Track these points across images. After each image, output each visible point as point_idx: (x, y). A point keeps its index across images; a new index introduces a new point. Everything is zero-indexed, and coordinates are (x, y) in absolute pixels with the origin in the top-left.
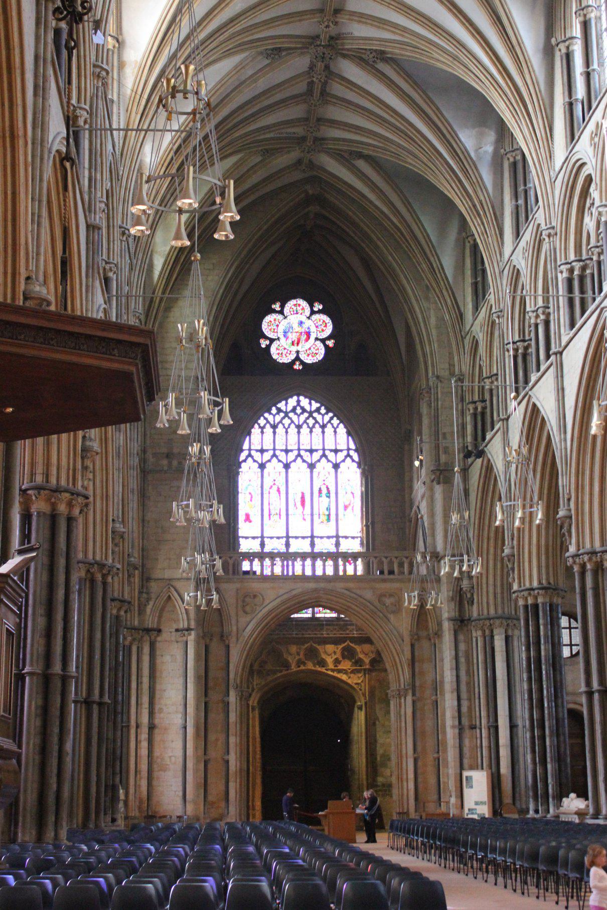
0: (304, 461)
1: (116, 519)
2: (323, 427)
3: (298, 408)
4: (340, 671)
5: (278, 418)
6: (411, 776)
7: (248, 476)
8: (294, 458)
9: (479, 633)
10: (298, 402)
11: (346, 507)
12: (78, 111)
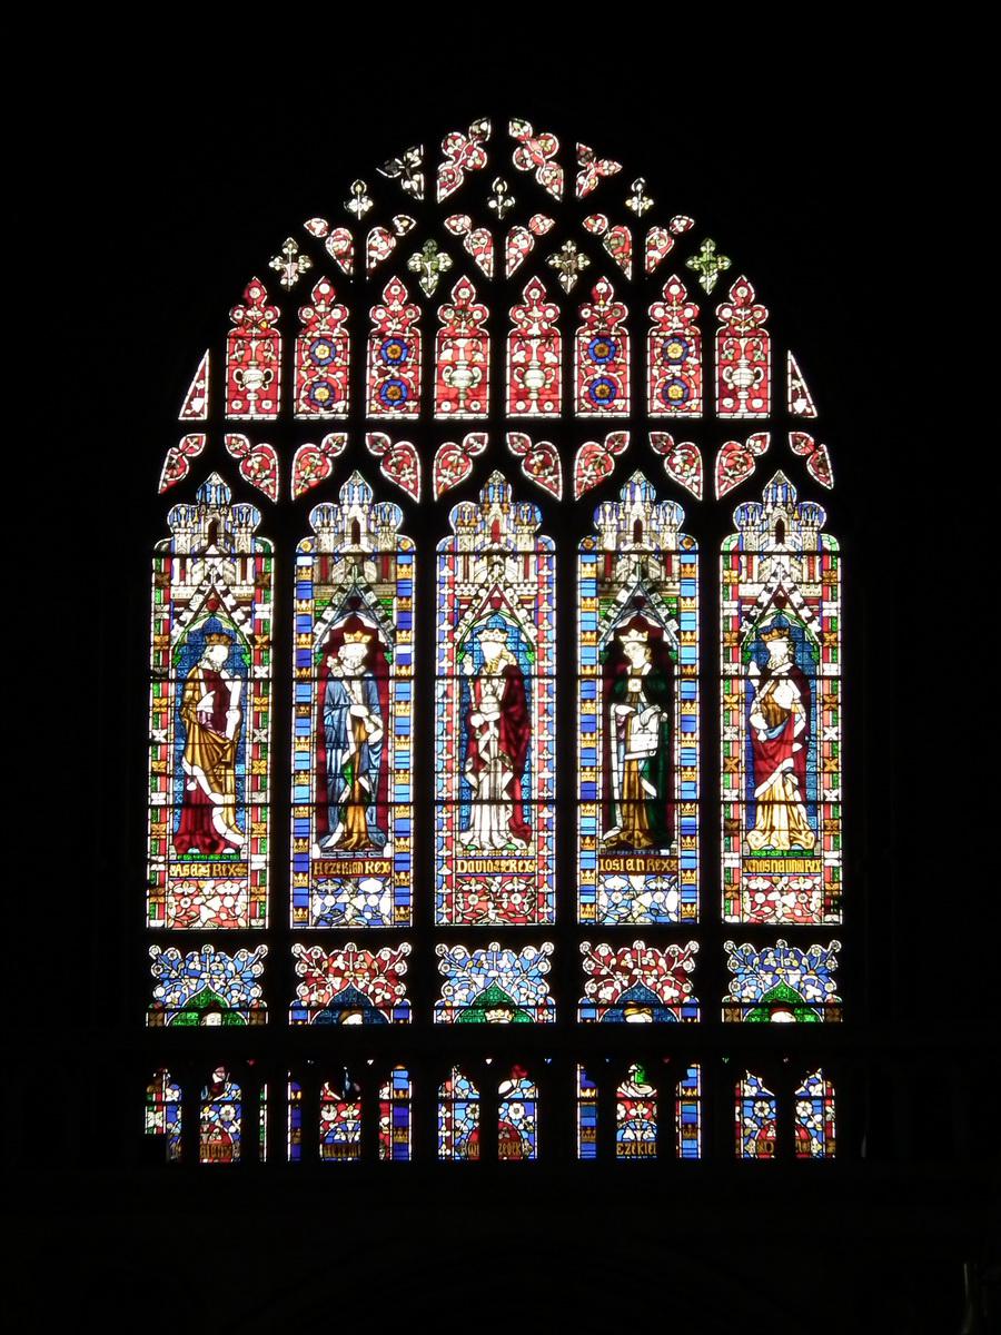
0: (525, 492)
2: (640, 292)
5: (380, 247)
10: (501, 147)
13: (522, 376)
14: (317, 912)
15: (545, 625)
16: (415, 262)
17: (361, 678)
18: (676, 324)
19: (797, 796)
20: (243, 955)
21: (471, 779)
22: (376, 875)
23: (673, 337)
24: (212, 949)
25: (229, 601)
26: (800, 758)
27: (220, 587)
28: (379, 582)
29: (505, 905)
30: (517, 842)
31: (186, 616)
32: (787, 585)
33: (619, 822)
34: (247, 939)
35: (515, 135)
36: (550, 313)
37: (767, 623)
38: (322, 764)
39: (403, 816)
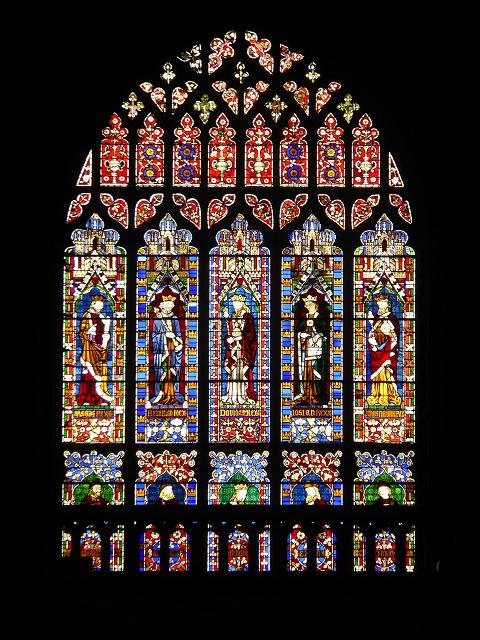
0: (255, 224)
2: (313, 122)
5: (179, 97)
10: (241, 46)
13: (252, 165)
14: (149, 435)
15: (265, 293)
16: (197, 106)
17: (171, 318)
18: (331, 138)
19: (393, 379)
20: (112, 456)
21: (228, 370)
22: (179, 417)
23: (330, 145)
24: (96, 453)
25: (103, 279)
26: (394, 360)
27: (99, 272)
28: (180, 270)
29: (244, 432)
30: (251, 401)
31: (82, 286)
32: (388, 272)
33: (302, 391)
34: (114, 448)
35: (248, 40)
36: (267, 133)
37: (378, 291)
38: (151, 361)
39: (193, 388)
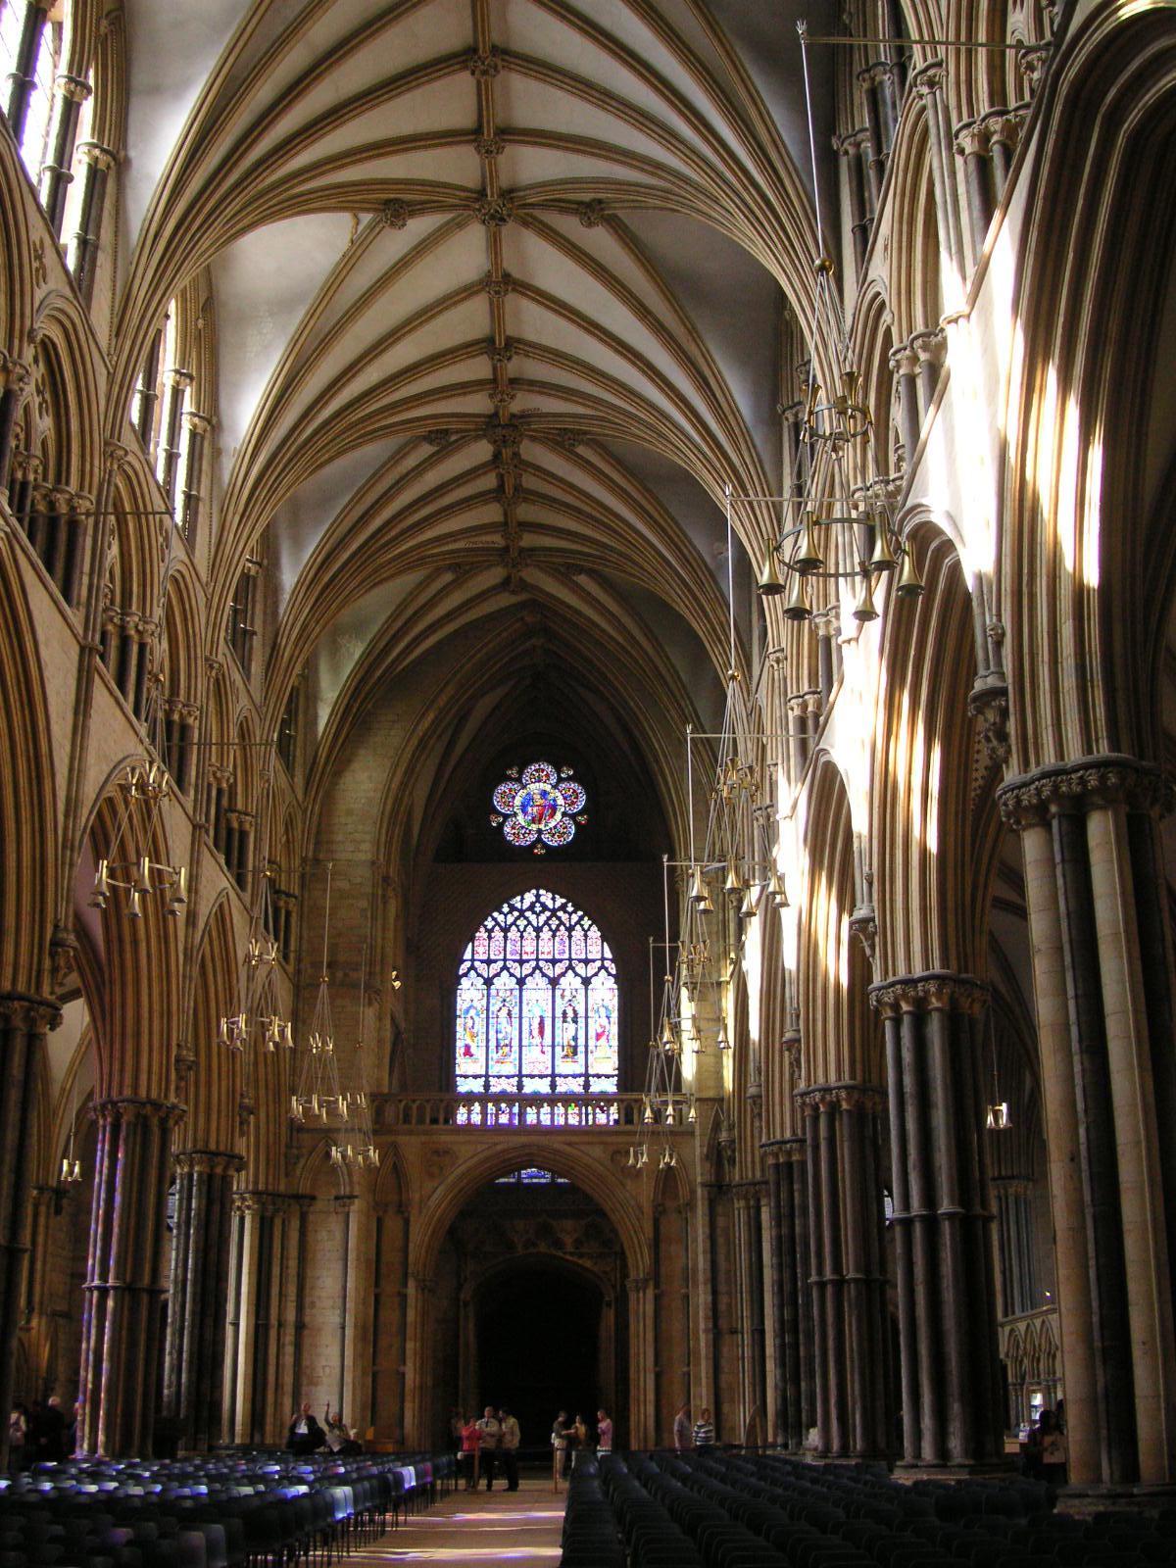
0: (544, 975)
1: (183, 1044)
2: (570, 929)
3: (538, 905)
4: (581, 1256)
5: (510, 919)
6: (651, 1396)
7: (469, 993)
8: (530, 971)
9: (742, 1203)
10: (538, 896)
11: (598, 1036)
12: (76, 500)
39: (516, 1048)
